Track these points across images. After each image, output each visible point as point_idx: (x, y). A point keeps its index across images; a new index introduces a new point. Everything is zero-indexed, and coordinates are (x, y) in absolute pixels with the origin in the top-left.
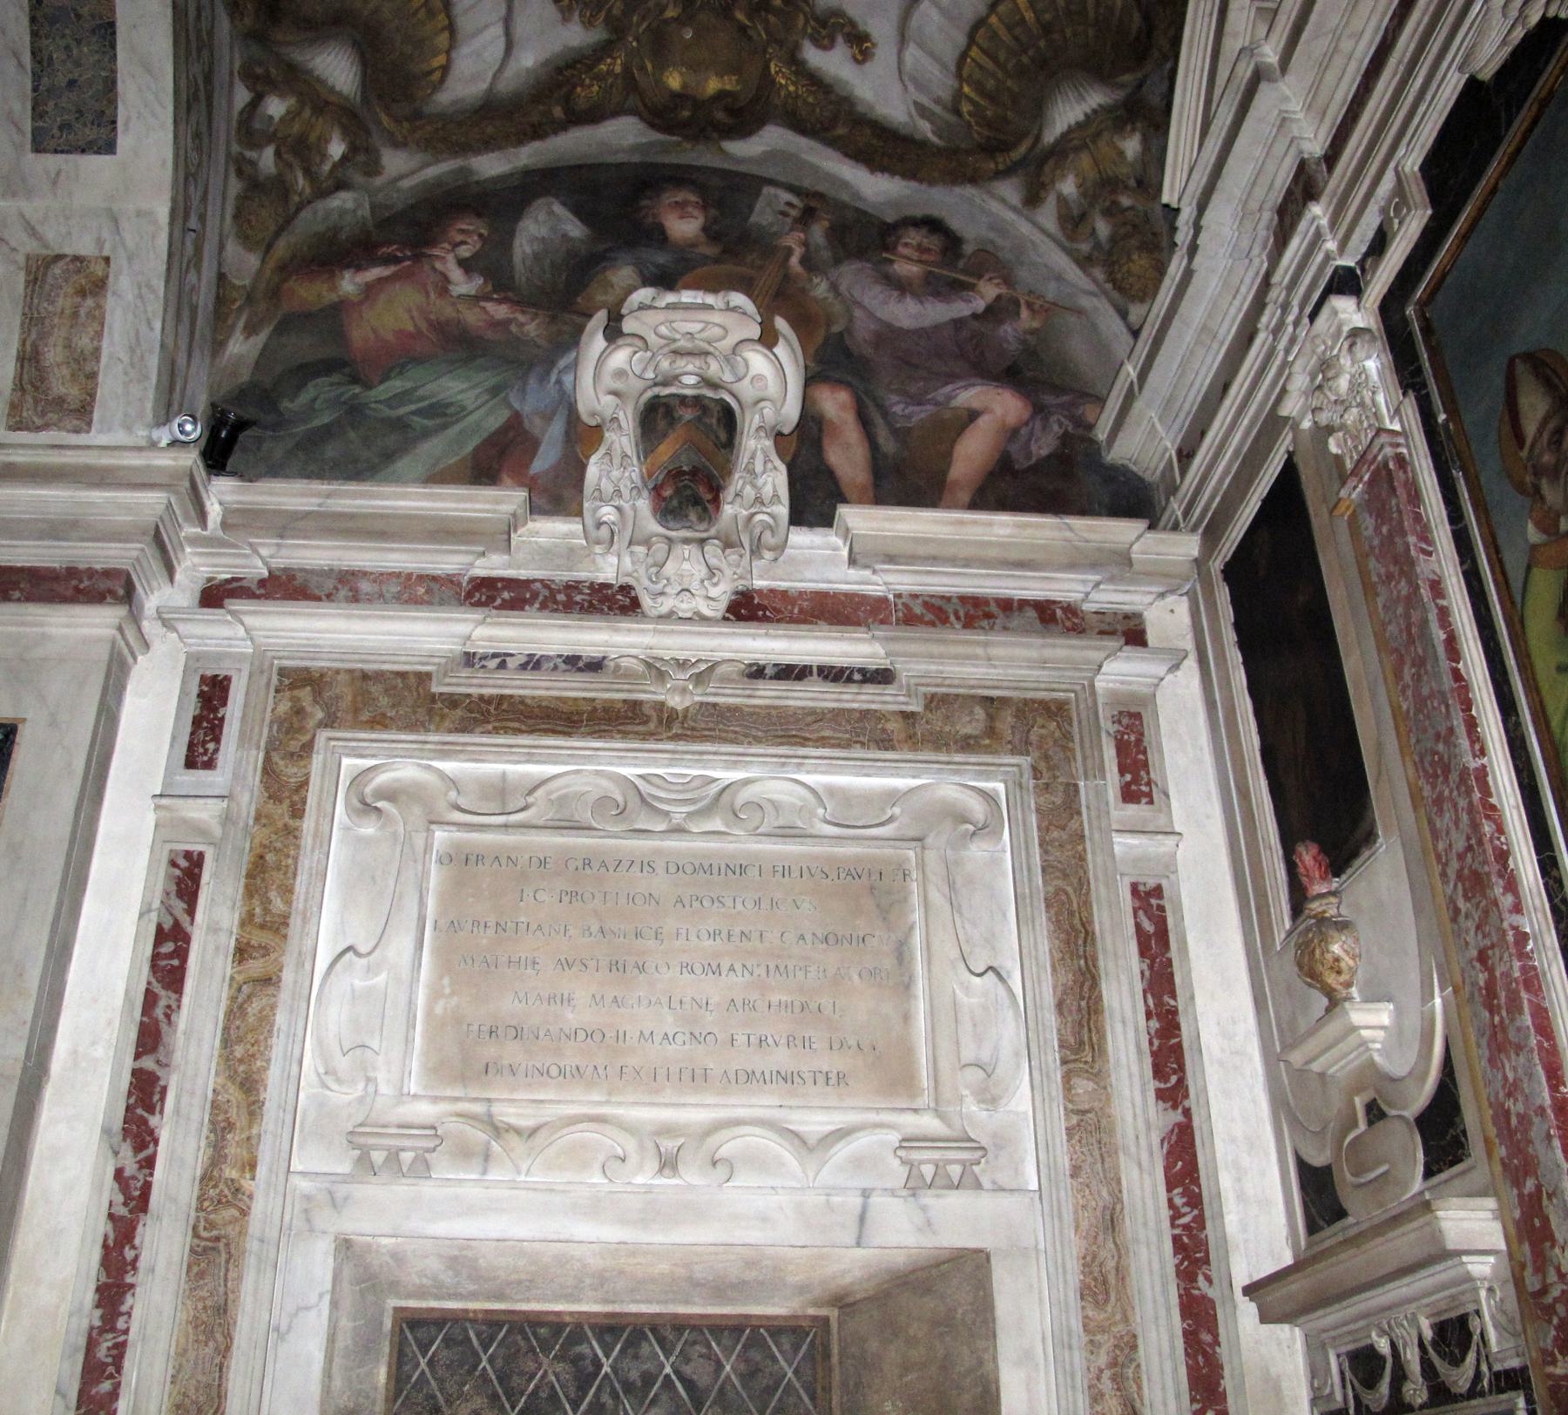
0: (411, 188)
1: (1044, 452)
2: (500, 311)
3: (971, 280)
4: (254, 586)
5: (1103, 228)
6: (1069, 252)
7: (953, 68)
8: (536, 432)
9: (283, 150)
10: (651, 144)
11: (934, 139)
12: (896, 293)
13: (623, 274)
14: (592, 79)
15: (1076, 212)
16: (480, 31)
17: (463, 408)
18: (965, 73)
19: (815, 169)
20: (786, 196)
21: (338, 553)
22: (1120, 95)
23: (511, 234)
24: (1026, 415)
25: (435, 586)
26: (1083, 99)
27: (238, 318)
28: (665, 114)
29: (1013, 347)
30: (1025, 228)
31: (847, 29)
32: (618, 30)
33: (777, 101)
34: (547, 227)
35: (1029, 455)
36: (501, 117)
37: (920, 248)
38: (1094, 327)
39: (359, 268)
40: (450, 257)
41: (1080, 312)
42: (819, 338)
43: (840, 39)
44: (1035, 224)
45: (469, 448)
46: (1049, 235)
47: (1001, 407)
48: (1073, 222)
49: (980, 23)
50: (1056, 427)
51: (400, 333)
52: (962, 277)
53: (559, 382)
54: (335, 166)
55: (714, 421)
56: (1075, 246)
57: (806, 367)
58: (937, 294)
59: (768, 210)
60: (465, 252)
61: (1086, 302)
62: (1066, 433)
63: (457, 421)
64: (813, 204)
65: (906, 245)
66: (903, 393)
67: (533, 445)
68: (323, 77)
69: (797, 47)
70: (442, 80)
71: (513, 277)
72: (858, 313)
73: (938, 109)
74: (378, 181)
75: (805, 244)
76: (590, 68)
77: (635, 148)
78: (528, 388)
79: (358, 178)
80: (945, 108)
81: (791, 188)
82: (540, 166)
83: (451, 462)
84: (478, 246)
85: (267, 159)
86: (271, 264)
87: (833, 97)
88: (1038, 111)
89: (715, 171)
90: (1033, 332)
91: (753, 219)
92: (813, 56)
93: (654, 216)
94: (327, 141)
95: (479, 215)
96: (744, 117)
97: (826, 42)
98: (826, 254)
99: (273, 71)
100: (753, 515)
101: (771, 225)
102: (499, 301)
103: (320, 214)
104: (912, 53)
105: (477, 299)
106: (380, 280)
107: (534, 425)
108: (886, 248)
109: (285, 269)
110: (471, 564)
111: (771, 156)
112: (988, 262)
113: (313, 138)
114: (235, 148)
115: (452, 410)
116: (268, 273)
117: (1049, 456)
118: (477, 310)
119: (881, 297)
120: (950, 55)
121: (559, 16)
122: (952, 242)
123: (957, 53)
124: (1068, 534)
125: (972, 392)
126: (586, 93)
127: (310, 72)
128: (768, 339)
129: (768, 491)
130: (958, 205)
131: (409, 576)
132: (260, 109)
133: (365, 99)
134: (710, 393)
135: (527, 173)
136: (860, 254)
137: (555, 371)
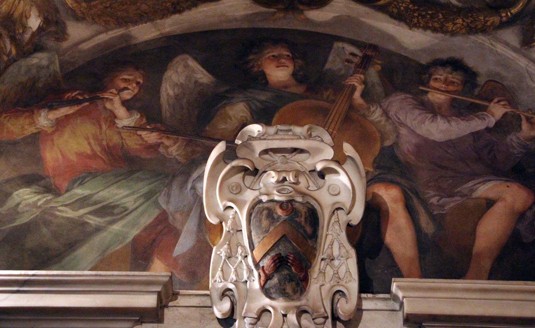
0: (89, 49)
2: (152, 137)
8: (178, 225)
10: (256, 14)
12: (430, 116)
13: (238, 109)
17: (126, 209)
30: (523, 62)
34: (185, 75)
37: (446, 82)
39: (51, 108)
40: (117, 99)
42: (376, 149)
51: (80, 155)
53: (193, 188)
54: (33, 35)
55: (303, 219)
57: (367, 173)
59: (338, 59)
60: (127, 95)
63: (121, 219)
64: (369, 53)
65: (436, 79)
67: (176, 234)
72: (403, 131)
74: (65, 45)
75: (365, 83)
78: (172, 193)
79: (51, 43)
81: (353, 42)
82: (178, 32)
83: (118, 248)
84: (136, 91)
89: (300, 32)
91: (328, 66)
93: (259, 66)
94: (27, 18)
95: (137, 68)
98: (379, 89)
101: (340, 70)
103: (23, 70)
107: (176, 220)
111: (338, 20)
112: (498, 89)
113: (16, 15)
115: (116, 211)
118: (136, 137)
119: (419, 118)
122: (470, 75)
136: (403, 89)
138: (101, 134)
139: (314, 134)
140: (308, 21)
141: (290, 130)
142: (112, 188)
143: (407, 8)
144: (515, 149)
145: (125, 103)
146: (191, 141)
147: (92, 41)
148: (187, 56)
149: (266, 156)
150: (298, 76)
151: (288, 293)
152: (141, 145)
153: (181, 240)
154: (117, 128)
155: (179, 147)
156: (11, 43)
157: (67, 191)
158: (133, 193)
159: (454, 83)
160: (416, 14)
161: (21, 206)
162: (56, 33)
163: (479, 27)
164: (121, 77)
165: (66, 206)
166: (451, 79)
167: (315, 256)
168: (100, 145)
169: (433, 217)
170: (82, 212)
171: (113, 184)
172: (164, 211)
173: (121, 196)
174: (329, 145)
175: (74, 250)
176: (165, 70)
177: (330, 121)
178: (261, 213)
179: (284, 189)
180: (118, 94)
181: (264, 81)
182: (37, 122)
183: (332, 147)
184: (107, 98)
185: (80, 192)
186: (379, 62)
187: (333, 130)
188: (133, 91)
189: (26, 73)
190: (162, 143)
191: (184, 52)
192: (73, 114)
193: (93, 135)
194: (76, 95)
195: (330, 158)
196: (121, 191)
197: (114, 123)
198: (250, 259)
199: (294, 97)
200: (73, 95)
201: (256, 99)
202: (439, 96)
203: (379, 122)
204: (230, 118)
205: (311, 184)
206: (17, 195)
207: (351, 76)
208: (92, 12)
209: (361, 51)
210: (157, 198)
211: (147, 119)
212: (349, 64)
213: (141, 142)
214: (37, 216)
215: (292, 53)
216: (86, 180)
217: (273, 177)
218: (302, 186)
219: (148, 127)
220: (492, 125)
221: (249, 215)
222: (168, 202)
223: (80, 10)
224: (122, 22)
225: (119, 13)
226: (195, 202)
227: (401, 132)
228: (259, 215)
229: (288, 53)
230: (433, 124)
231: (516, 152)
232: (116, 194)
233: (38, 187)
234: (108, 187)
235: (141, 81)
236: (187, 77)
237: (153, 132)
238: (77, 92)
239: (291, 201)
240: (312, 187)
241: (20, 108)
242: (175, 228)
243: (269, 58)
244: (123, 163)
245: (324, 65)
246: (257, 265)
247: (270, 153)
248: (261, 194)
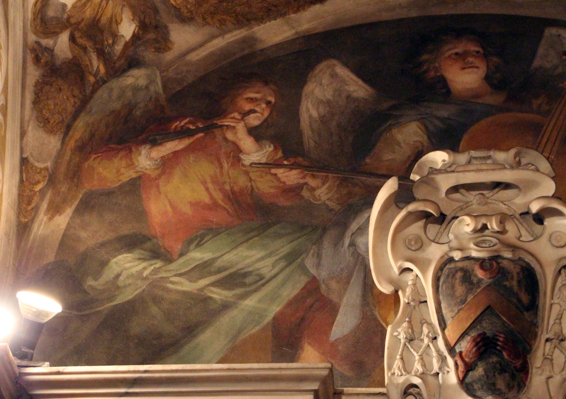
2: (291, 177)
8: (334, 297)
9: (77, 34)
13: (410, 133)
17: (261, 277)
27: (42, 199)
34: (331, 88)
39: (154, 143)
40: (240, 127)
51: (195, 205)
53: (352, 244)
54: (126, 45)
55: (515, 283)
60: (254, 120)
63: (256, 291)
67: (332, 310)
74: (169, 56)
79: (149, 55)
82: (320, 29)
83: (254, 331)
84: (266, 114)
85: (62, 45)
86: (72, 144)
91: (537, 63)
93: (436, 69)
94: (118, 23)
95: (266, 83)
102: (291, 167)
103: (115, 93)
109: (86, 149)
113: (104, 20)
114: (32, 38)
115: (248, 280)
118: (269, 177)
135: (308, 38)
137: (349, 233)
138: (222, 174)
139: (524, 161)
141: (489, 157)
142: (240, 249)
145: (252, 131)
146: (345, 179)
147: (203, 48)
148: (335, 62)
149: (457, 196)
151: (499, 389)
152: (277, 187)
153: (340, 318)
154: (243, 165)
155: (330, 189)
156: (98, 58)
157: (181, 255)
158: (270, 255)
161: (121, 278)
162: (156, 41)
164: (245, 96)
165: (180, 275)
167: (535, 336)
168: (222, 190)
170: (202, 283)
171: (241, 243)
172: (314, 278)
173: (254, 259)
174: (547, 175)
175: (195, 336)
176: (305, 83)
177: (545, 140)
178: (454, 276)
179: (484, 241)
180: (242, 119)
182: (136, 164)
183: (553, 178)
184: (227, 126)
185: (197, 255)
187: (550, 154)
188: (262, 114)
189: (119, 97)
190: (306, 183)
193: (212, 178)
194: (186, 124)
195: (551, 193)
196: (254, 252)
197: (239, 160)
198: (440, 342)
199: (490, 110)
200: (182, 124)
204: (399, 144)
205: (523, 232)
206: (116, 263)
208: (203, 10)
210: (303, 260)
211: (283, 152)
213: (276, 183)
214: (144, 290)
215: (483, 47)
216: (206, 239)
217: (468, 225)
218: (511, 234)
219: (285, 163)
221: (436, 280)
222: (318, 265)
223: (187, 8)
225: (239, 9)
226: (356, 263)
228: (450, 280)
229: (477, 49)
232: (247, 257)
233: (143, 252)
234: (236, 248)
235: (272, 99)
236: (335, 91)
237: (292, 169)
238: (188, 120)
239: (496, 258)
240: (526, 236)
241: (113, 146)
242: (331, 301)
243: (449, 56)
244: (254, 214)
245: (531, 62)
246: (451, 350)
247: (462, 191)
248: (452, 249)
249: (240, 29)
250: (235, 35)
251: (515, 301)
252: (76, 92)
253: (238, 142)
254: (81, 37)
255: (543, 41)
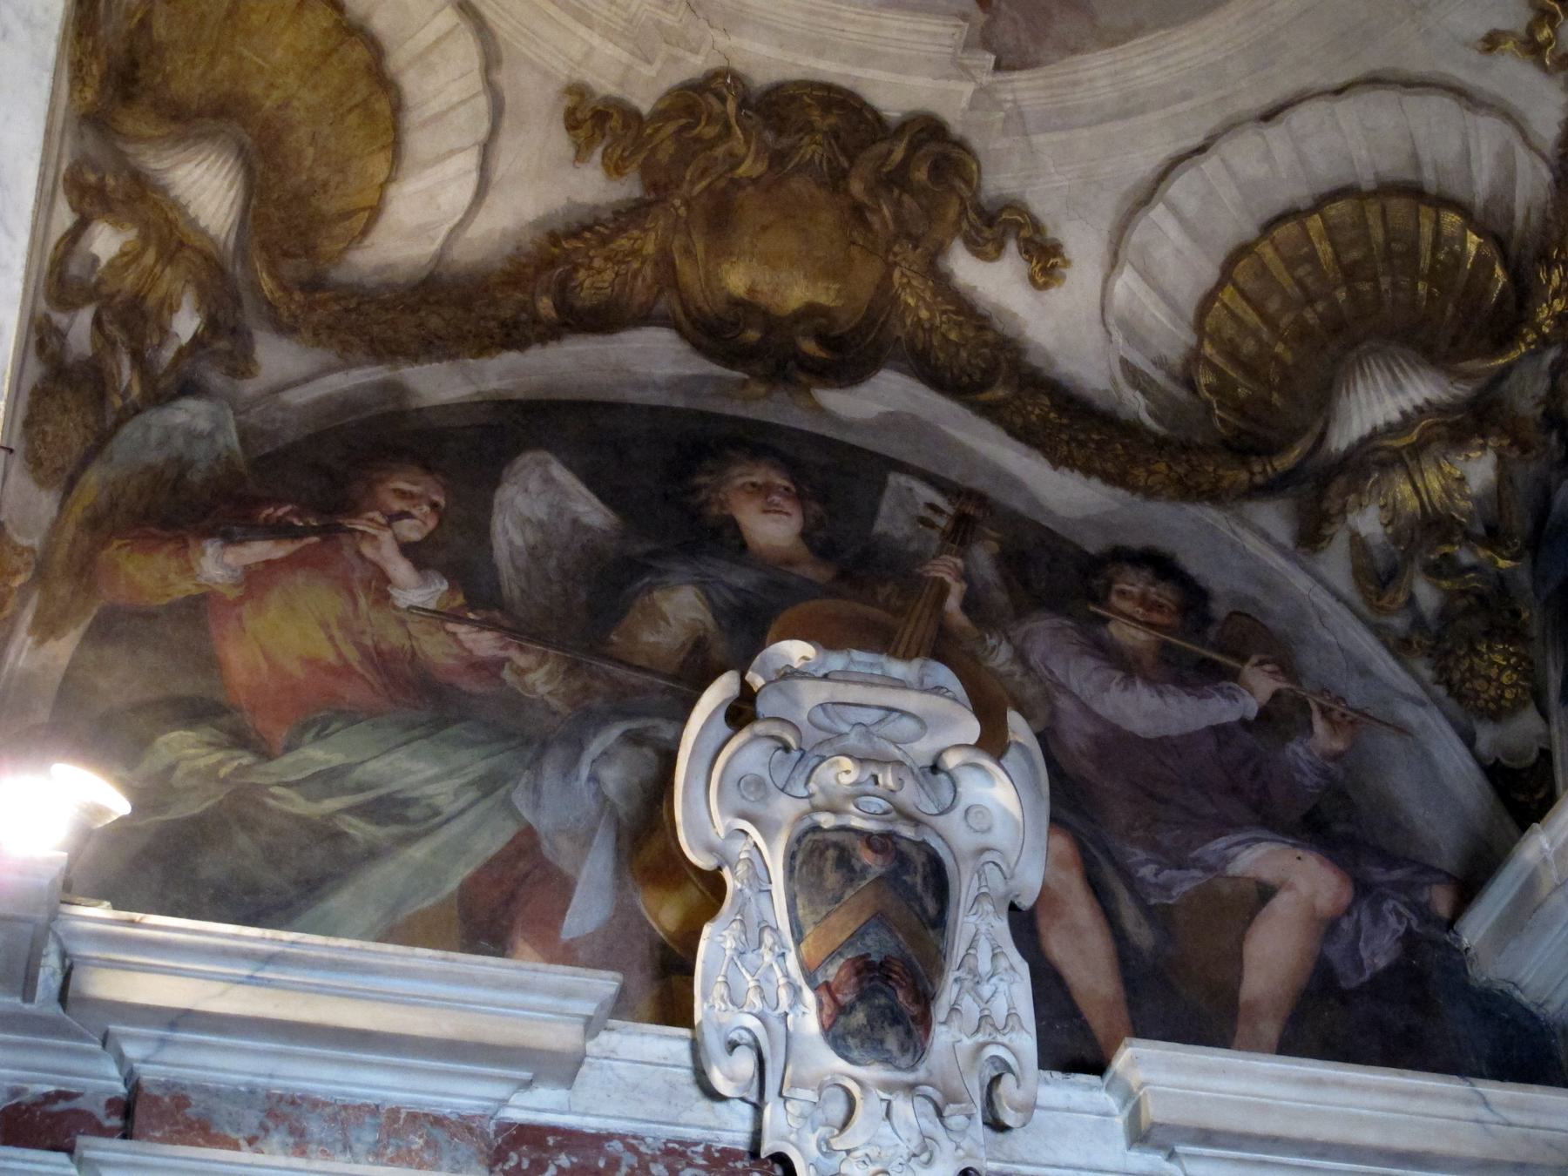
1: (1381, 962)
2: (484, 643)
3: (1231, 663)
4: (100, 1112)
5: (1427, 595)
6: (1377, 630)
7: (1190, 314)
8: (565, 864)
10: (703, 379)
11: (1149, 422)
12: (1119, 675)
14: (607, 259)
15: (1381, 565)
16: (440, 159)
17: (437, 813)
18: (1210, 323)
19: (967, 454)
20: (926, 493)
21: (266, 1065)
22: (1463, 390)
23: (488, 507)
24: (1346, 896)
25: (440, 1135)
26: (1401, 388)
27: (23, 604)
28: (717, 331)
29: (1310, 779)
30: (1301, 583)
31: (1025, 233)
32: (659, 187)
33: (899, 332)
35: (1359, 966)
36: (458, 306)
37: (1143, 600)
38: (1426, 756)
39: (229, 539)
41: (1402, 730)
43: (1012, 246)
44: (1320, 580)
45: (452, 885)
46: (1339, 597)
47: (1305, 882)
48: (1377, 579)
49: (1243, 251)
50: (1392, 919)
51: (311, 662)
52: (1216, 657)
54: (181, 352)
55: (919, 880)
56: (1383, 620)
58: (1181, 682)
60: (411, 530)
61: (1409, 714)
62: (1409, 931)
63: (427, 833)
64: (970, 510)
65: (1122, 593)
66: (1154, 846)
67: (565, 888)
68: (183, 201)
69: (941, 249)
70: (365, 232)
71: (498, 587)
72: (1064, 703)
73: (1159, 376)
74: (250, 387)
75: (965, 576)
76: (604, 241)
77: (677, 384)
80: (1172, 376)
82: (519, 396)
83: (426, 904)
86: (77, 512)
87: (990, 336)
88: (1324, 401)
90: (1337, 757)
91: (880, 526)
92: (965, 268)
93: (722, 504)
94: (173, 310)
95: (428, 469)
96: (848, 352)
97: (990, 248)
98: (1000, 598)
99: (110, 181)
100: (983, 1046)
101: (909, 540)
102: (482, 625)
103: (155, 435)
104: (1126, 283)
105: (441, 616)
106: (269, 563)
108: (1095, 599)
110: (504, 1103)
111: (891, 422)
115: (413, 813)
116: (69, 531)
117: (1390, 970)
118: (441, 636)
120: (1189, 293)
121: (570, 152)
122: (1194, 597)
123: (1199, 294)
124: (1482, 1112)
125: (1261, 850)
126: (594, 283)
127: (164, 190)
128: (993, 742)
129: (1000, 1008)
130: (1195, 532)
131: (394, 1112)
132: (83, 243)
133: (241, 248)
134: (907, 831)
135: (501, 405)
136: (1053, 603)
140: (820, 411)
142: (393, 757)
143: (1044, 419)
144: (1305, 774)
145: (408, 550)
148: (548, 456)
150: (816, 540)
151: (889, 1051)
152: (456, 657)
153: (577, 901)
154: (395, 607)
155: (550, 674)
156: (133, 367)
157: (288, 749)
158: (450, 774)
159: (1161, 606)
160: (1064, 437)
161: (178, 774)
162: (230, 354)
163: (1206, 487)
164: (392, 486)
165: (287, 785)
166: (1155, 597)
168: (359, 645)
169: (1151, 913)
170: (330, 805)
171: (398, 746)
173: (421, 777)
175: (321, 898)
176: (495, 483)
178: (822, 854)
180: (389, 525)
181: (737, 542)
182: (197, 570)
184: (363, 533)
185: (319, 755)
186: (993, 534)
188: (425, 523)
189: (161, 444)
190: (508, 659)
191: (538, 445)
192: (282, 560)
194: (286, 514)
195: (973, 741)
196: (421, 765)
197: (388, 596)
198: (792, 962)
199: (808, 590)
200: (280, 513)
201: (722, 582)
202: (1133, 631)
203: (1011, 675)
204: (665, 618)
206: (167, 744)
207: (934, 557)
208: (315, 318)
209: (950, 502)
210: (509, 793)
211: (466, 597)
212: (928, 530)
213: (456, 650)
214: (221, 802)
215: (795, 483)
216: (332, 729)
217: (847, 772)
219: (471, 616)
220: (1252, 714)
221: (791, 856)
222: (537, 806)
223: (289, 309)
224: (385, 350)
225: (376, 329)
226: (600, 815)
227: (1059, 704)
228: (815, 860)
229: (786, 483)
230: (1128, 695)
231: (1307, 782)
232: (409, 772)
233: (215, 731)
234: (388, 752)
235: (441, 501)
236: (551, 506)
238: (288, 508)
241: (153, 530)
242: (560, 872)
243: (743, 486)
244: (423, 699)
246: (810, 977)
248: (816, 809)
249: (378, 364)
250: (361, 377)
251: (917, 908)
252: (91, 419)
253: (382, 563)
254: (111, 323)
255: (888, 493)
